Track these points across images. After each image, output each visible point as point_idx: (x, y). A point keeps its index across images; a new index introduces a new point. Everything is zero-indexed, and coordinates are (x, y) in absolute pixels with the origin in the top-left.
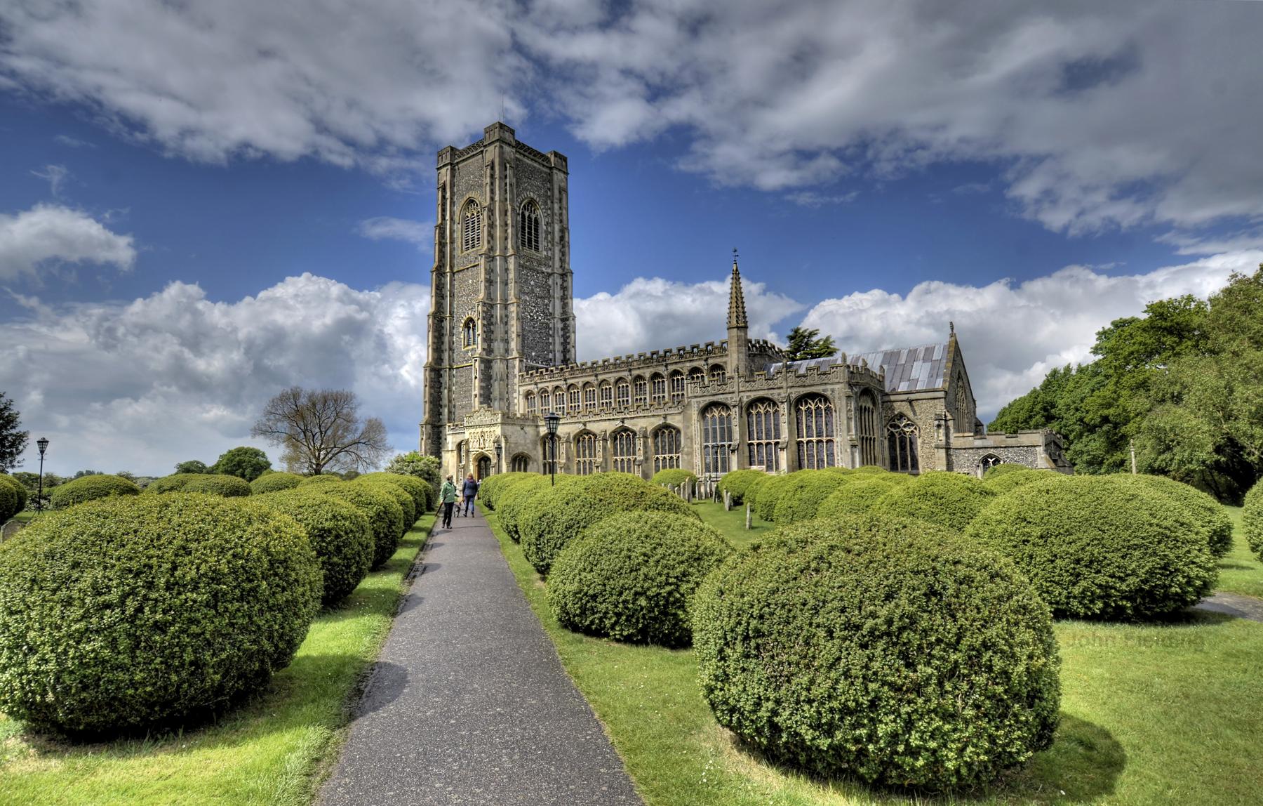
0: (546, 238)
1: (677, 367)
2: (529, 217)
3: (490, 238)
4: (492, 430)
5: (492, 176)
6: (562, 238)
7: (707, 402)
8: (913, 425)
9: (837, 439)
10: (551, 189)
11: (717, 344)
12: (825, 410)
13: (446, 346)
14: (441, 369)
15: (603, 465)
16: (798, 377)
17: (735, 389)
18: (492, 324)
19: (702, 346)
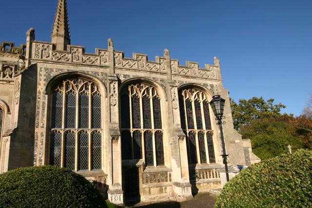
7: (66, 71)
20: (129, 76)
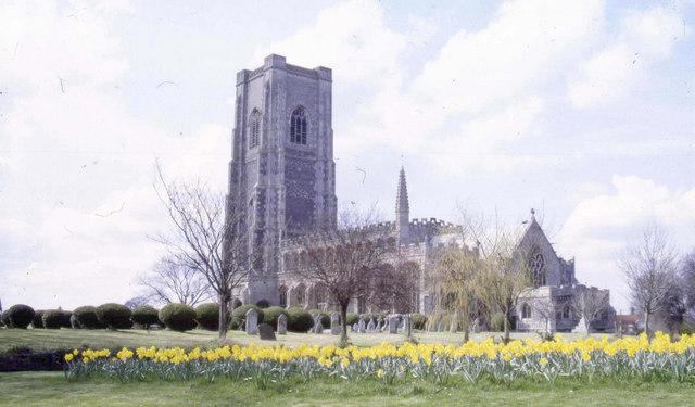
6: (325, 133)
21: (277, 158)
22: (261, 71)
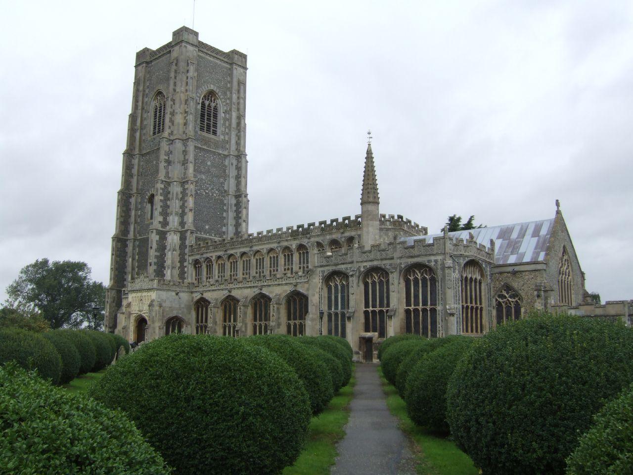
0: (224, 124)
1: (319, 239)
2: (209, 106)
3: (170, 124)
4: (149, 294)
5: (176, 71)
6: (239, 124)
8: (517, 296)
9: (439, 308)
10: (231, 82)
11: (353, 218)
12: (431, 280)
13: (132, 219)
14: (127, 240)
15: (243, 329)
16: (406, 248)
17: (355, 259)
18: (169, 199)
19: (340, 220)
20: (366, 266)
21: (185, 145)
22: (167, 49)
